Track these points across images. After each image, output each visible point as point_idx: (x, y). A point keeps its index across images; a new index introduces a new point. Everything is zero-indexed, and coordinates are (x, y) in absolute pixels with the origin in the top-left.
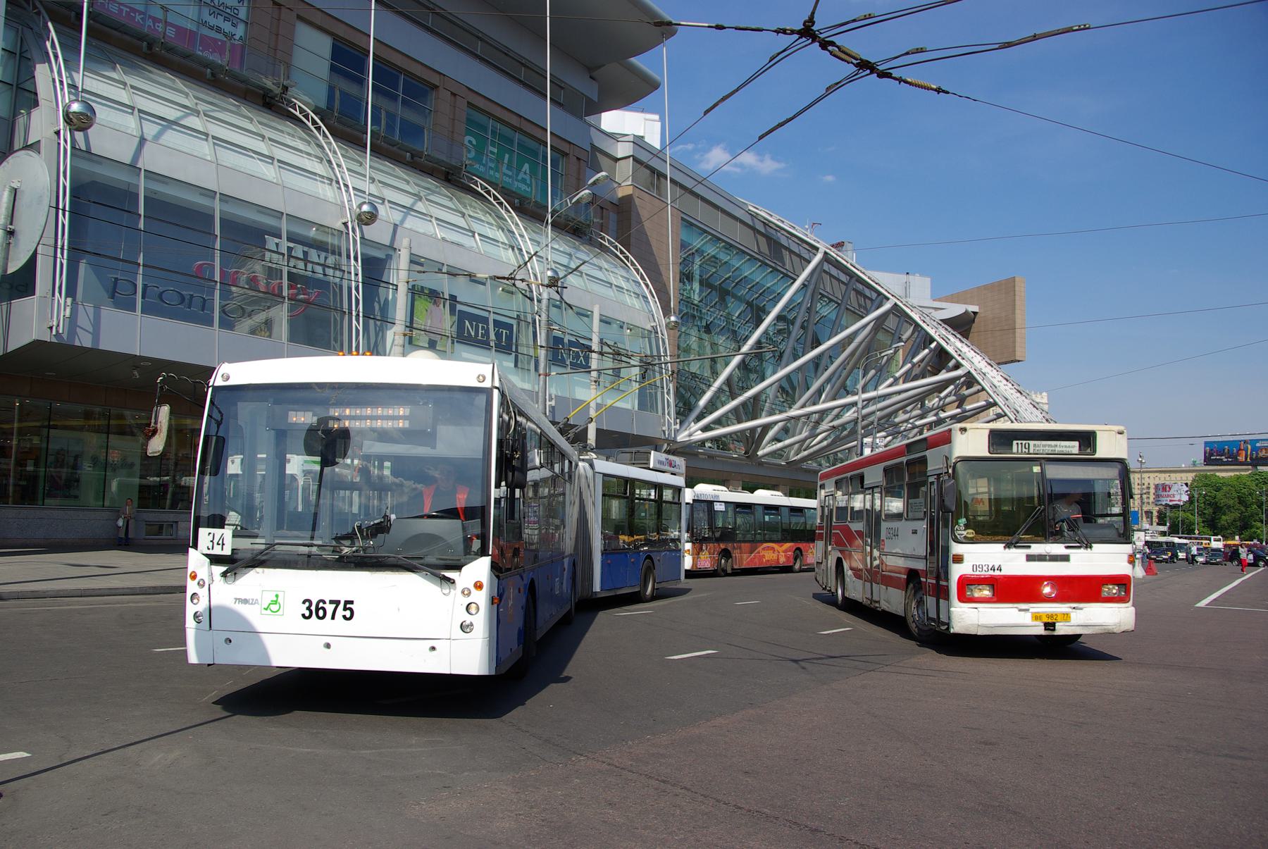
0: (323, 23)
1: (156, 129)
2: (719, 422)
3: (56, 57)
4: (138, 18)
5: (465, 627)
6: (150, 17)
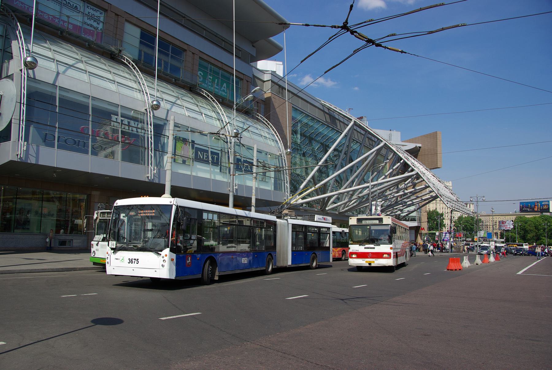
1: (64, 68)
2: (309, 195)
3: (21, 38)
4: (57, 21)
5: (163, 266)
6: (62, 20)
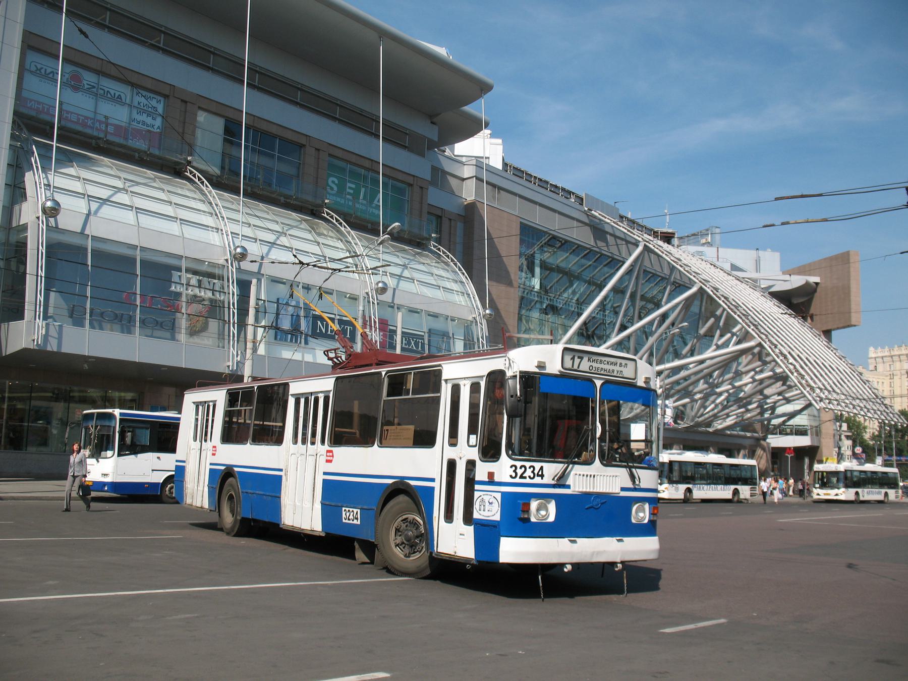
0: (215, 108)
3: (37, 167)
4: (90, 123)
